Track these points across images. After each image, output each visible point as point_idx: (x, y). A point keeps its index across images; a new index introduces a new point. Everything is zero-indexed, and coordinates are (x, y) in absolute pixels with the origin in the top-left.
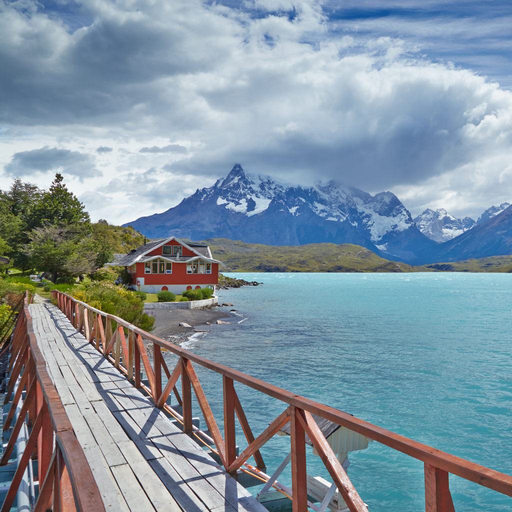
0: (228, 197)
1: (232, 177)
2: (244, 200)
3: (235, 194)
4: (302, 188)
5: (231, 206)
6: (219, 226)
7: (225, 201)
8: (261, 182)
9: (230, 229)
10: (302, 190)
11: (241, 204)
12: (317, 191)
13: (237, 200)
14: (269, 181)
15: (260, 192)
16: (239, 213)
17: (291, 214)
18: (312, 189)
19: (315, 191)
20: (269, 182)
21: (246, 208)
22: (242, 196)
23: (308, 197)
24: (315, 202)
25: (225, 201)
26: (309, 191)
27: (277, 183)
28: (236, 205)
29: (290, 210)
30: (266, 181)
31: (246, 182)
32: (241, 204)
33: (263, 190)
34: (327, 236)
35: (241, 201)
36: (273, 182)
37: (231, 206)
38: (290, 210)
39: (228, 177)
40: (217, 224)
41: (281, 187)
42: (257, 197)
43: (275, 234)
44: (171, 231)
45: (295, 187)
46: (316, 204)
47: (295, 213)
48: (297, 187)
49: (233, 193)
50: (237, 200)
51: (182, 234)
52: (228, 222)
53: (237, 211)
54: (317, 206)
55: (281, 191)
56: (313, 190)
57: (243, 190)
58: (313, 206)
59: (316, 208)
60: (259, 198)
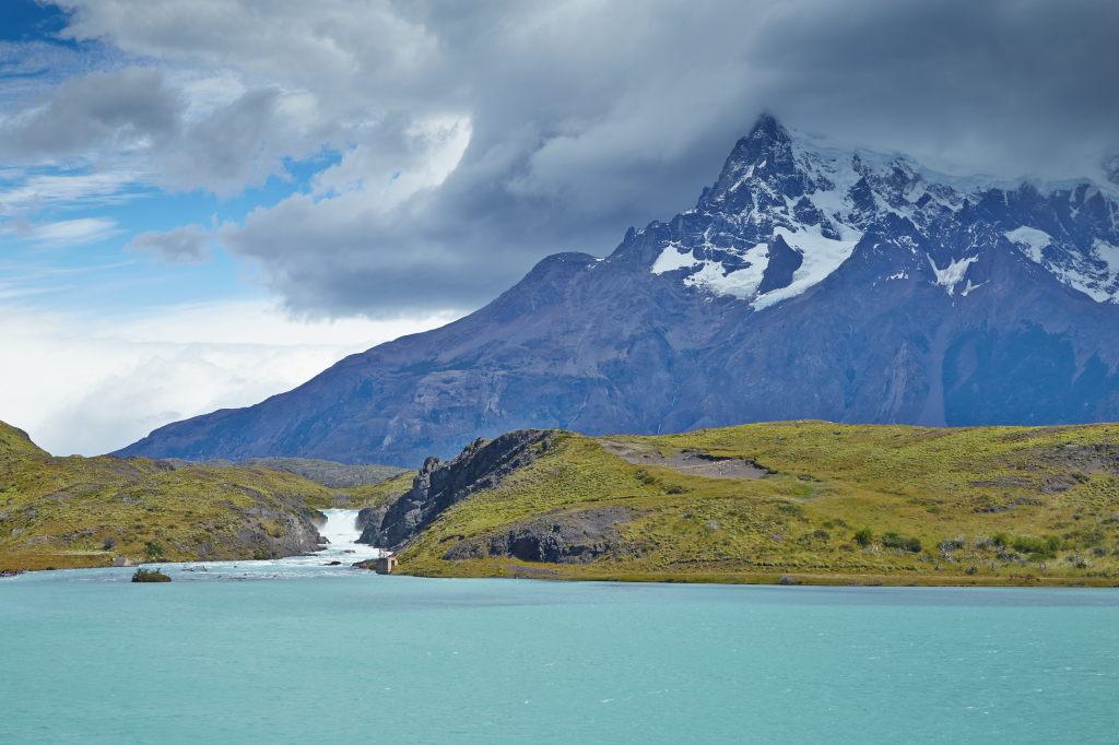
0: (703, 241)
1: (736, 169)
2: (763, 248)
3: (730, 228)
4: (1042, 191)
5: (712, 276)
6: (623, 355)
7: (688, 260)
8: (855, 178)
9: (670, 363)
10: (1042, 198)
11: (748, 265)
12: (1104, 192)
13: (733, 250)
14: (898, 172)
15: (851, 218)
16: (729, 299)
17: (943, 288)
18: (1083, 188)
19: (1098, 198)
20: (900, 179)
21: (759, 278)
22: (750, 236)
23: (1068, 223)
24: (1097, 241)
25: (688, 260)
26: (1072, 198)
27: (931, 180)
28: (730, 270)
29: (940, 274)
30: (884, 171)
31: (795, 186)
32: (748, 265)
33: (863, 209)
34: (1077, 375)
35: (746, 258)
36: (918, 178)
37: (712, 276)
38: (940, 274)
39: (727, 167)
40: (619, 347)
41: (948, 192)
42: (826, 235)
43: (851, 375)
44: (423, 381)
45: (1005, 188)
46: (1103, 250)
47: (959, 286)
48: (1015, 187)
49: (722, 224)
50: (733, 250)
51: (469, 389)
52: (669, 336)
53: (722, 292)
54: (1103, 258)
55: (945, 209)
56: (1089, 194)
57: (761, 209)
58: (1089, 259)
59: (1102, 264)
60: (838, 238)
